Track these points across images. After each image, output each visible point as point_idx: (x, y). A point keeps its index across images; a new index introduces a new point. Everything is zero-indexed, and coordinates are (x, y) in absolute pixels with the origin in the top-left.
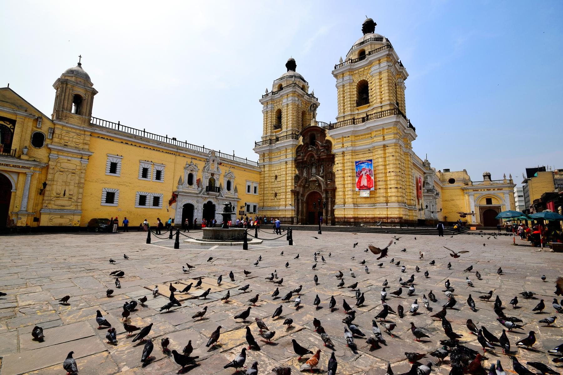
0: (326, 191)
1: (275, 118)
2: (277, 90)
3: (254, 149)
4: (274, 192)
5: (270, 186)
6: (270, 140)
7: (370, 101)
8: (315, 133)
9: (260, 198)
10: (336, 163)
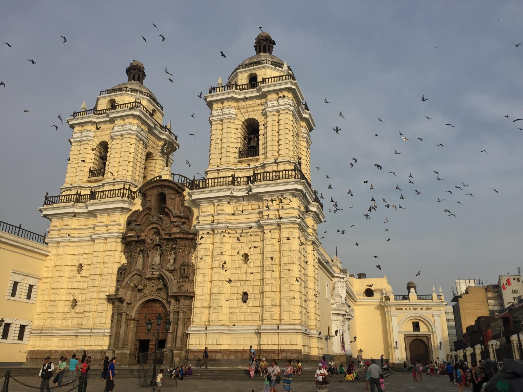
2: (105, 108)
4: (72, 299)
6: (79, 195)
8: (167, 191)
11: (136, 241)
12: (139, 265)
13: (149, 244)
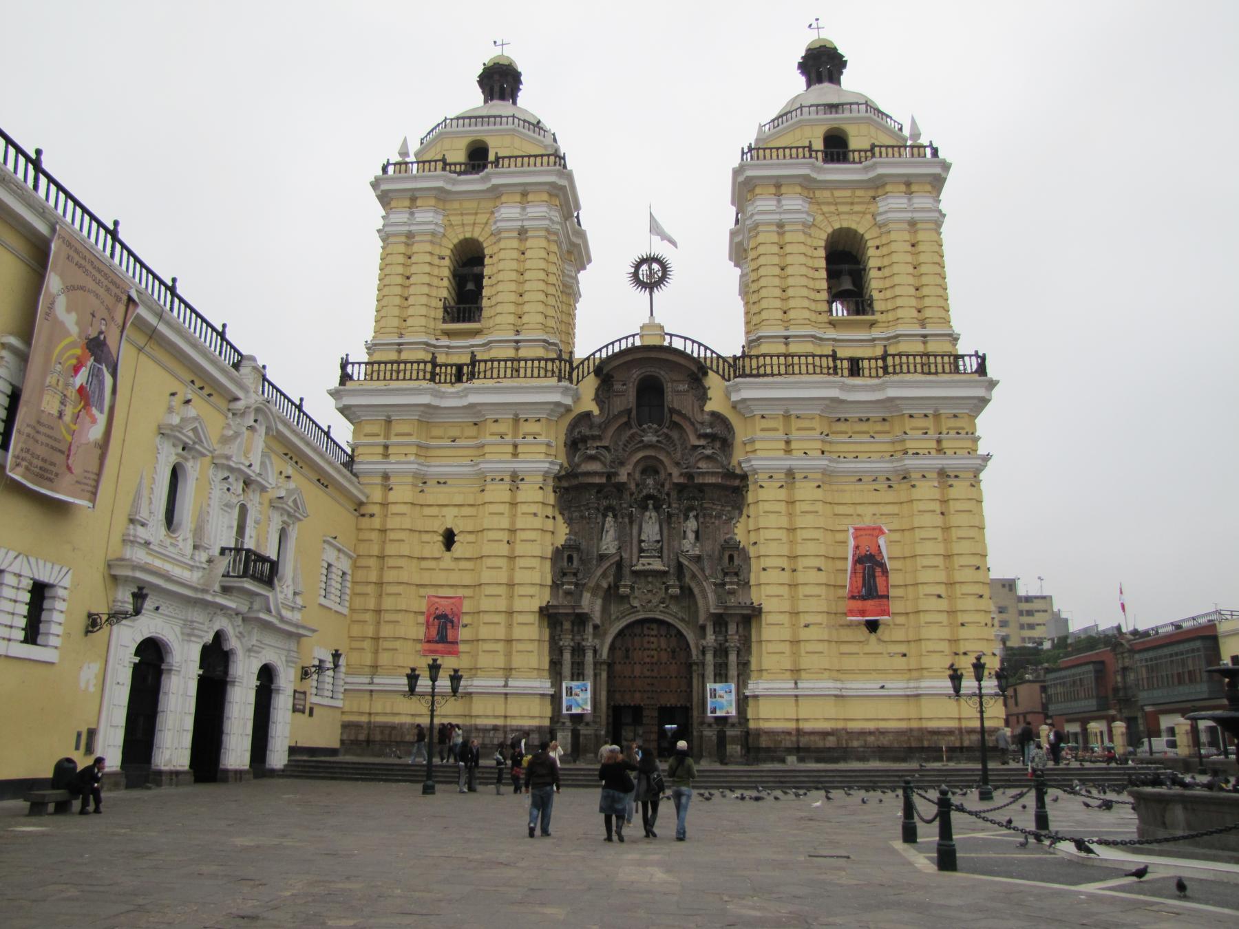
0: (720, 622)
1: (446, 272)
3: (334, 394)
5: (416, 579)
6: (434, 364)
7: (878, 306)
9: (356, 631)
10: (752, 510)
11: (600, 488)
12: (609, 544)
13: (632, 494)
